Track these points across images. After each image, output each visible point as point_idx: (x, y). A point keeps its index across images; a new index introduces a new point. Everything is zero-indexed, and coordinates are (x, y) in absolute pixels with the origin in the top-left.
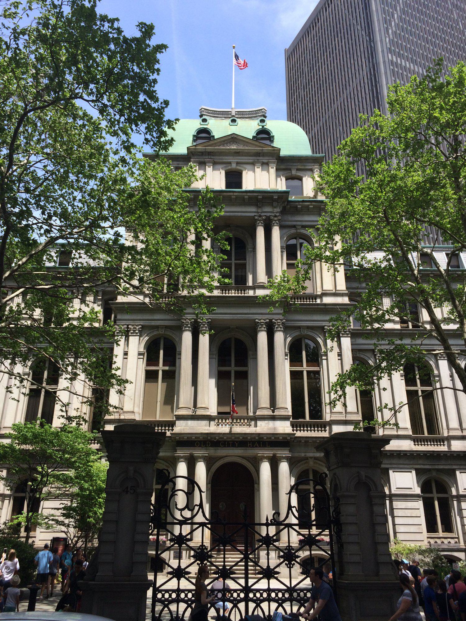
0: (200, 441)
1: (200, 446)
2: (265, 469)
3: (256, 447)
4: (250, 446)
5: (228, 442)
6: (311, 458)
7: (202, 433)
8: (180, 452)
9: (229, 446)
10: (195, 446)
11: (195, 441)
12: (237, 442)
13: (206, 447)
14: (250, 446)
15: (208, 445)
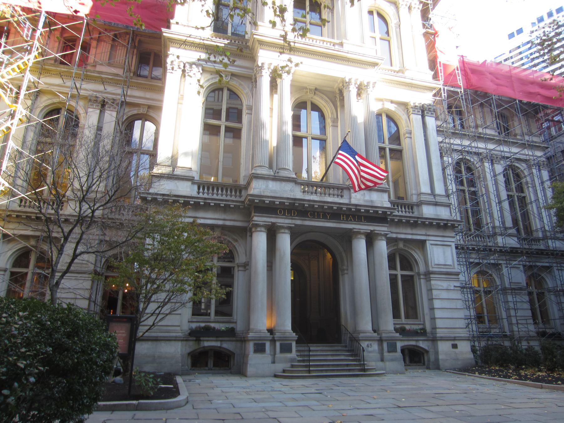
0: (284, 210)
1: (284, 214)
2: (360, 245)
3: (351, 220)
4: (343, 219)
5: (318, 212)
6: (401, 239)
7: (288, 199)
8: (258, 219)
9: (319, 217)
10: (277, 214)
11: (278, 209)
12: (328, 213)
13: (291, 215)
14: (343, 219)
15: (294, 214)
